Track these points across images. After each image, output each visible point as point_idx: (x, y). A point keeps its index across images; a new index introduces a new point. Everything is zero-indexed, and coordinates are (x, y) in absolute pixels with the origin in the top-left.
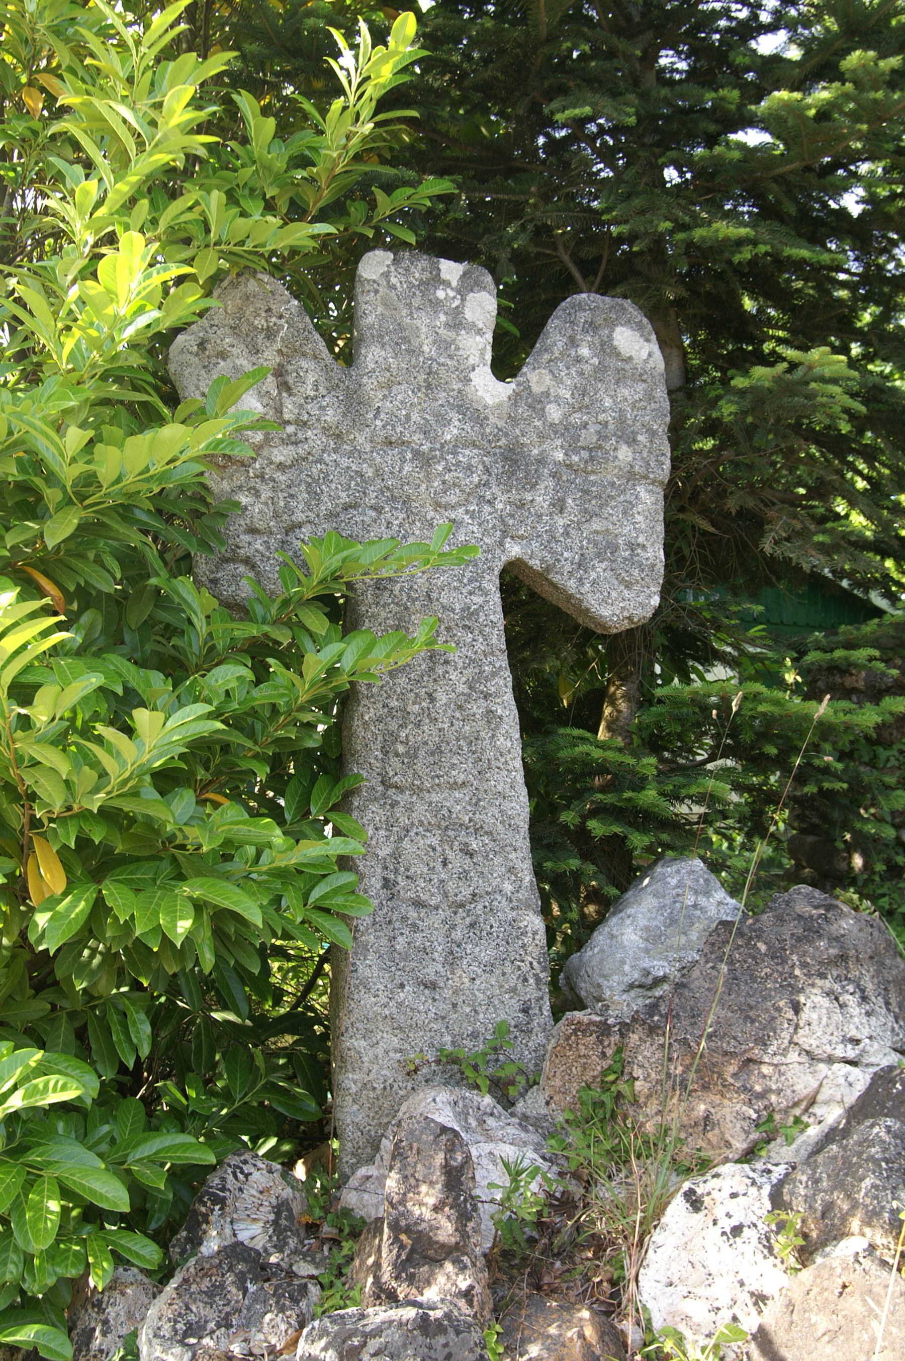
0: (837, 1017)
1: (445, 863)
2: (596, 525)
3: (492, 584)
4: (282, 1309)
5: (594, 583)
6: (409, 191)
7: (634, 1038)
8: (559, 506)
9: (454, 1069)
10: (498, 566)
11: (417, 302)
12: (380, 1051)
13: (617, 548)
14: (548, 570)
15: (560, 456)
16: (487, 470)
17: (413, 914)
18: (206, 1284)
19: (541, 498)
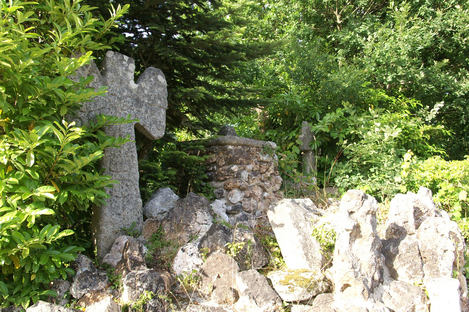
0: (203, 216)
1: (122, 188)
2: (153, 117)
3: (133, 128)
4: (103, 281)
5: (153, 129)
6: (116, 38)
7: (164, 222)
8: (146, 112)
9: (124, 232)
10: (134, 124)
11: (119, 64)
12: (108, 229)
13: (157, 122)
14: (144, 125)
15: (147, 101)
16: (132, 103)
17: (116, 199)
18: (83, 279)
19: (143, 110)
